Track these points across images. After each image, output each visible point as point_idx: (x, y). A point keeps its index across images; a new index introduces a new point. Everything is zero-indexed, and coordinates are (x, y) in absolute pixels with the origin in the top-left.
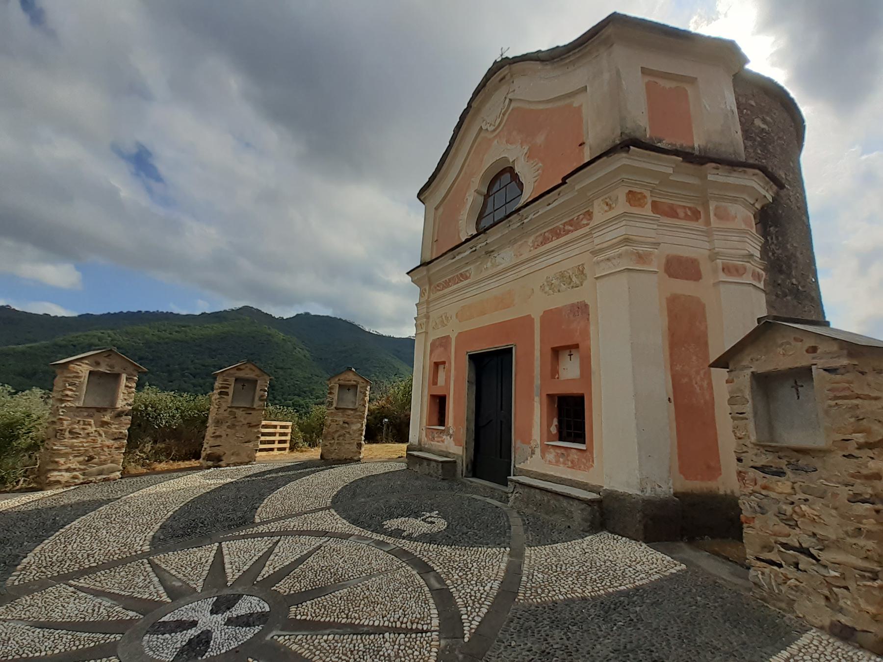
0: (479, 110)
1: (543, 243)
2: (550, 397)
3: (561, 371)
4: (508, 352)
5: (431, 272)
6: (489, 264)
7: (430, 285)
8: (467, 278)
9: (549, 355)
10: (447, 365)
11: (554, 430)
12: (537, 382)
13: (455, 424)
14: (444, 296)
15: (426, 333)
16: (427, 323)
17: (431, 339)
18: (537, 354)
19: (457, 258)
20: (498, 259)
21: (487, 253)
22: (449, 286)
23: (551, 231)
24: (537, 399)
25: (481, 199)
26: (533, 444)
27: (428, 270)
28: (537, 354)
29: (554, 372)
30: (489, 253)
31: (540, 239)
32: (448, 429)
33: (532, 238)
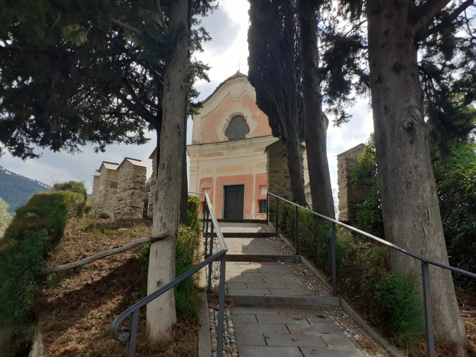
0: (229, 84)
1: (258, 151)
2: (258, 200)
4: (244, 185)
5: (202, 148)
6: (234, 152)
7: (199, 153)
8: (222, 155)
9: (258, 187)
10: (211, 189)
11: (258, 210)
12: (254, 195)
15: (197, 175)
16: (198, 170)
17: (200, 178)
18: (254, 187)
19: (219, 146)
20: (238, 152)
22: (211, 156)
23: (260, 148)
25: (228, 123)
26: (252, 215)
28: (254, 187)
29: (260, 193)
30: (234, 148)
31: (256, 149)
33: (253, 148)
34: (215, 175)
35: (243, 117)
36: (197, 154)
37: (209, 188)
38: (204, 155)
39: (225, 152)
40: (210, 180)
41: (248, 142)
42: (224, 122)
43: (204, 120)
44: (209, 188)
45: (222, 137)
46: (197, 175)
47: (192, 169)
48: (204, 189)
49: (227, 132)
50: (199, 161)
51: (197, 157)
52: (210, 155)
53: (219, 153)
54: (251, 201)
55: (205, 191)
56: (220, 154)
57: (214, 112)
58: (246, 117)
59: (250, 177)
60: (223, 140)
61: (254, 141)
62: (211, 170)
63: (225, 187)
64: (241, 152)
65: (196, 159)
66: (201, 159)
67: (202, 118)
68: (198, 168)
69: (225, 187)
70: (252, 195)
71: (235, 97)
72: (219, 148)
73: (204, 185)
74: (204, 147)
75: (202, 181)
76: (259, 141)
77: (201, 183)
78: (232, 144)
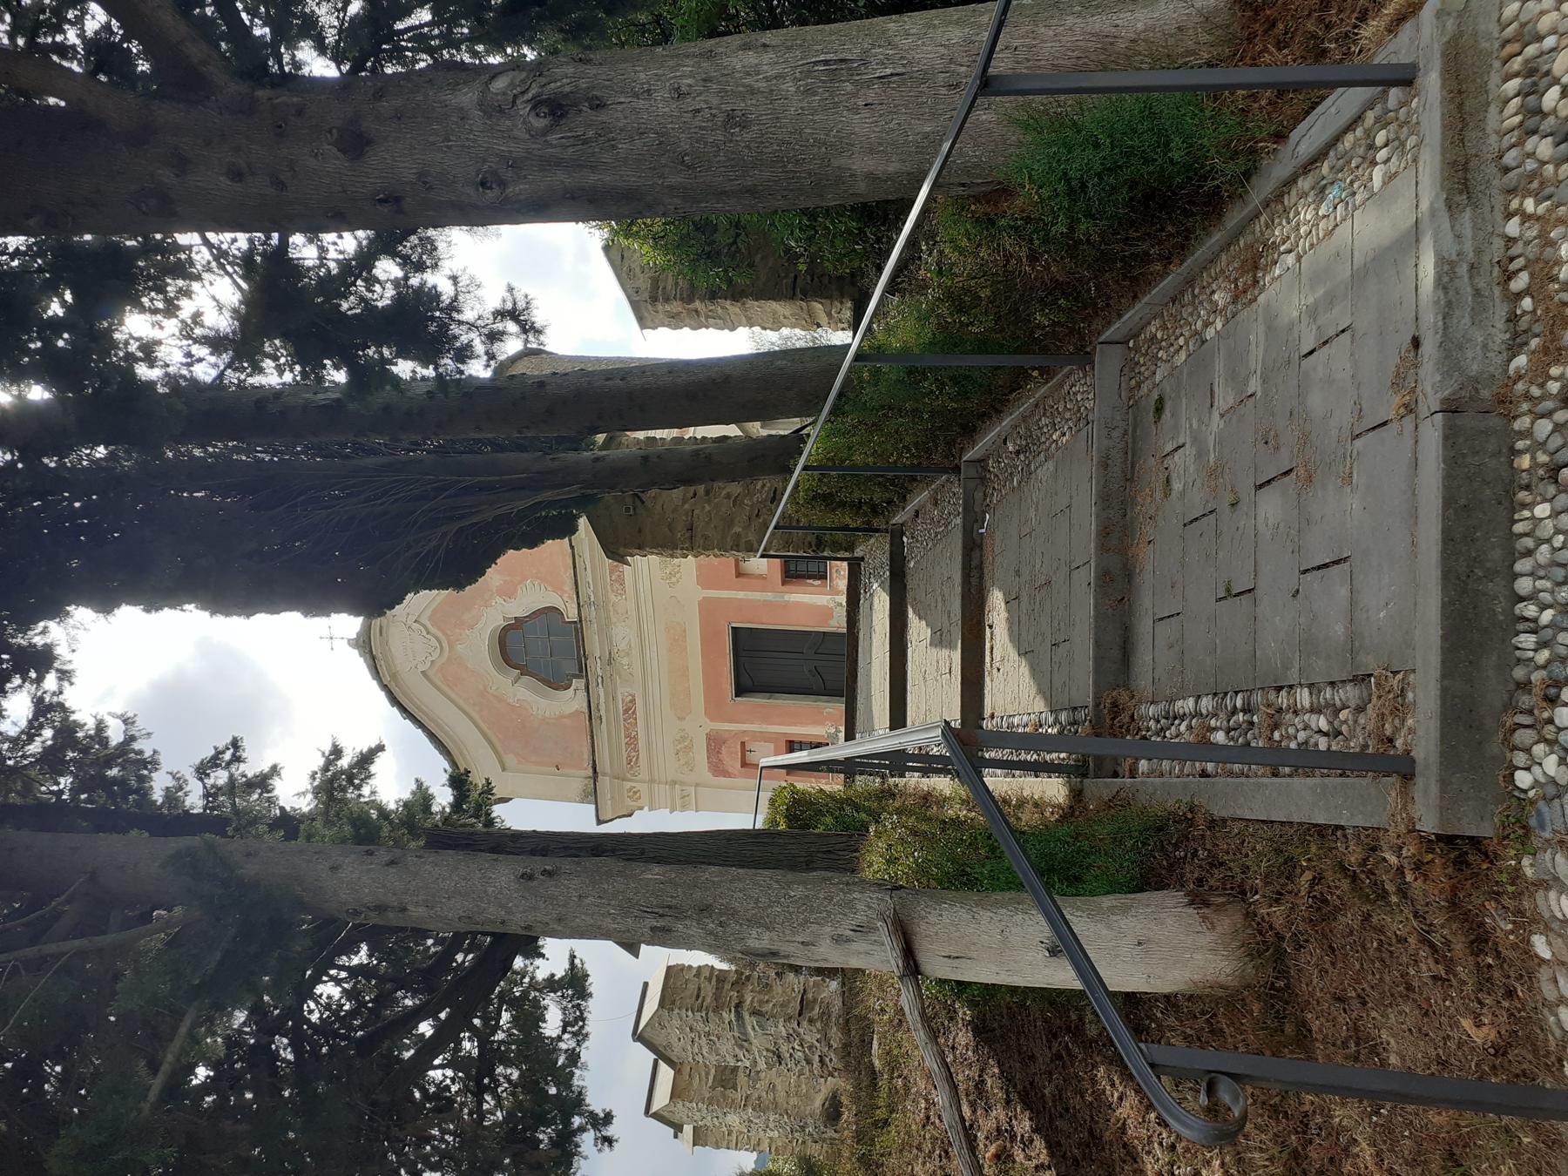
0: (394, 676)
1: (622, 583)
3: (758, 572)
4: (736, 631)
5: (608, 770)
6: (625, 661)
8: (633, 701)
11: (818, 582)
12: (769, 596)
13: (821, 723)
14: (649, 743)
15: (697, 785)
16: (682, 783)
17: (708, 776)
18: (741, 595)
19: (603, 712)
20: (623, 646)
21: (610, 663)
22: (636, 738)
23: (611, 573)
24: (787, 597)
25: (526, 678)
26: (832, 605)
27: (605, 775)
28: (741, 595)
29: (761, 577)
32: (829, 735)
33: (613, 598)
34: (700, 726)
35: (505, 630)
36: (628, 785)
37: (743, 744)
38: (632, 762)
39: (622, 692)
40: (715, 744)
41: (590, 613)
42: (523, 694)
43: (510, 760)
44: (743, 744)
45: (571, 701)
46: (697, 785)
47: (678, 802)
48: (744, 764)
49: (557, 682)
50: (652, 781)
51: (638, 786)
52: (632, 741)
53: (626, 712)
54: (787, 605)
55: (751, 758)
56: (630, 710)
57: (484, 726)
58: (505, 619)
59: (707, 608)
60: (582, 694)
61: (587, 591)
62: (683, 738)
63: (740, 691)
64: (623, 635)
65: (643, 788)
66: (644, 775)
67: (504, 770)
68: (674, 783)
69: (740, 691)
70: (766, 604)
71: (436, 655)
72: (607, 711)
73: (733, 763)
74: (604, 764)
75: (718, 769)
76: (587, 577)
77: (726, 774)
78: (596, 667)
